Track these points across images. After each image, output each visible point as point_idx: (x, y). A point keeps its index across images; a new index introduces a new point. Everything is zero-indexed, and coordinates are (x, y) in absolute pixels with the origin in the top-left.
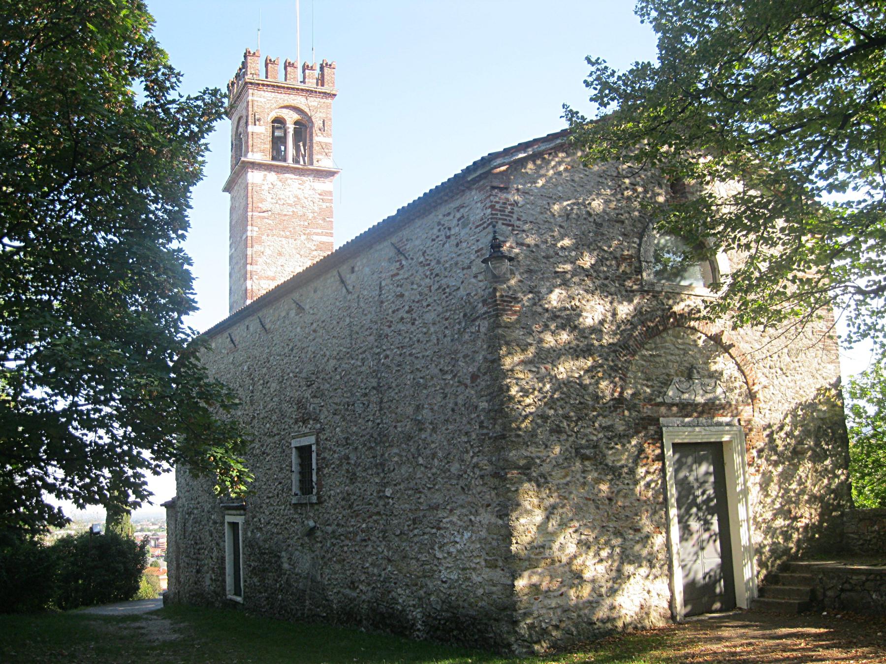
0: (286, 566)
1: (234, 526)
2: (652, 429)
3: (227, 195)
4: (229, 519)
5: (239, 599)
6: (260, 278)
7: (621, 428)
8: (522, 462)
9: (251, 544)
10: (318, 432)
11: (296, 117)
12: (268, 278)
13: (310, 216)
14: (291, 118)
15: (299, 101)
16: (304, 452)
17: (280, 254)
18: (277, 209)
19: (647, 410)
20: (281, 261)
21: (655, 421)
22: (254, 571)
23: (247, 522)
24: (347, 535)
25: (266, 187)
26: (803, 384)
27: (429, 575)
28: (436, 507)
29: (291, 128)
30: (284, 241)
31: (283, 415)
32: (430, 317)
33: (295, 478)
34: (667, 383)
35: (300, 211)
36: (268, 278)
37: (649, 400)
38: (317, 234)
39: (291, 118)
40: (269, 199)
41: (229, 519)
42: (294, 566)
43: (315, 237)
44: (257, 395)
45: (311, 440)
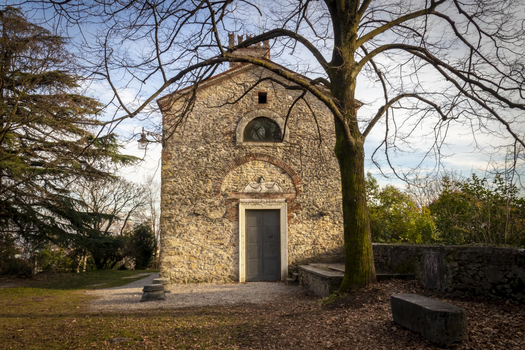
2: (234, 204)
7: (217, 203)
8: (167, 216)
19: (234, 196)
26: (331, 183)
37: (236, 192)
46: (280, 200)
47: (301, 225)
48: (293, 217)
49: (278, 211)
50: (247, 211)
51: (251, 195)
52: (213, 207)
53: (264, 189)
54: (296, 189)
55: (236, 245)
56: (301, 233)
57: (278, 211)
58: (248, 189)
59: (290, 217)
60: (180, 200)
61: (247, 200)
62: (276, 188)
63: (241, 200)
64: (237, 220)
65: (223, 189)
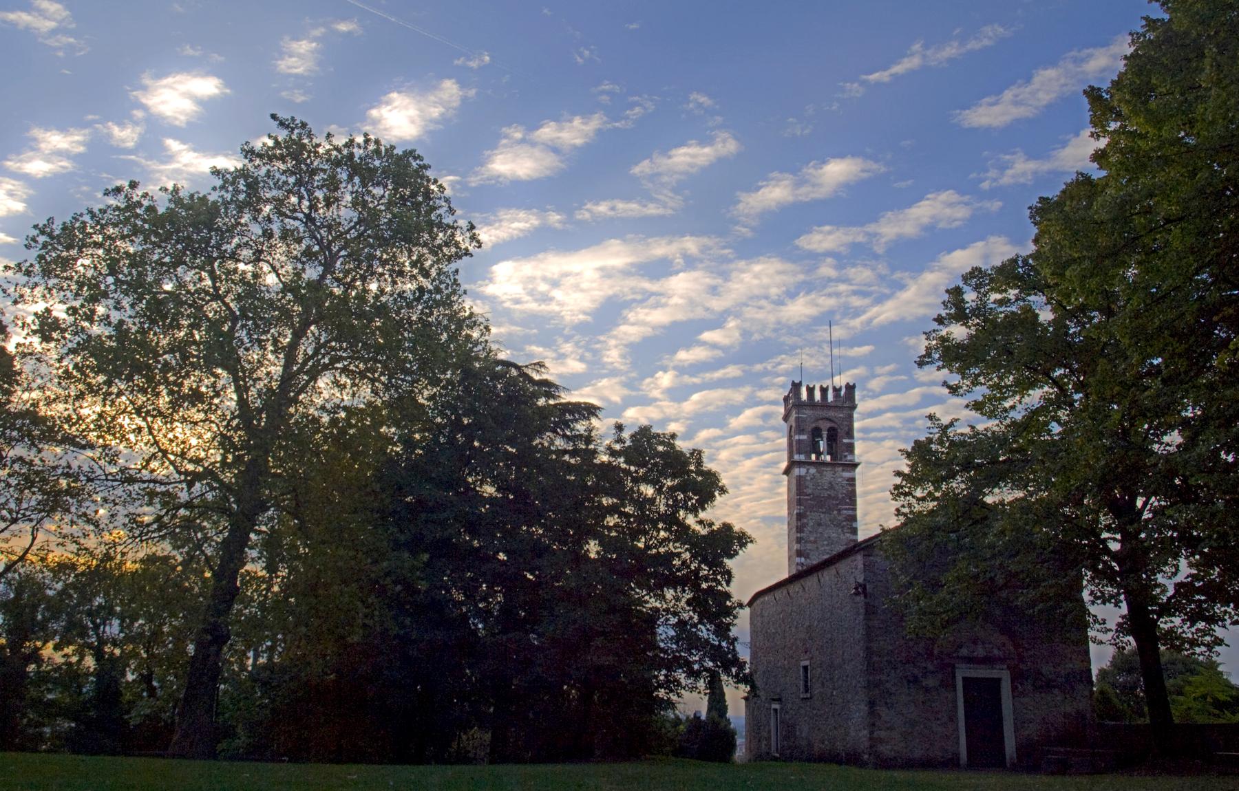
0: (798, 733)
1: (776, 710)
3: (785, 477)
5: (778, 755)
7: (931, 667)
9: (782, 722)
10: (812, 658)
11: (829, 425)
12: (811, 542)
13: (840, 496)
15: (831, 414)
16: (805, 668)
17: (820, 525)
19: (947, 661)
20: (820, 530)
21: (953, 667)
22: (786, 738)
25: (808, 478)
29: (825, 434)
30: (822, 516)
32: (847, 608)
33: (802, 683)
35: (832, 493)
36: (811, 542)
39: (825, 426)
40: (811, 486)
42: (801, 733)
44: (787, 634)
45: (807, 663)
46: (1001, 667)
47: (1026, 700)
48: (1017, 688)
49: (999, 680)
50: (964, 679)
51: (970, 660)
52: (926, 673)
53: (980, 652)
55: (953, 719)
56: (1026, 708)
57: (999, 680)
58: (964, 652)
59: (1014, 689)
60: (889, 662)
61: (964, 666)
62: (996, 652)
63: (957, 665)
64: (955, 690)
65: (936, 652)
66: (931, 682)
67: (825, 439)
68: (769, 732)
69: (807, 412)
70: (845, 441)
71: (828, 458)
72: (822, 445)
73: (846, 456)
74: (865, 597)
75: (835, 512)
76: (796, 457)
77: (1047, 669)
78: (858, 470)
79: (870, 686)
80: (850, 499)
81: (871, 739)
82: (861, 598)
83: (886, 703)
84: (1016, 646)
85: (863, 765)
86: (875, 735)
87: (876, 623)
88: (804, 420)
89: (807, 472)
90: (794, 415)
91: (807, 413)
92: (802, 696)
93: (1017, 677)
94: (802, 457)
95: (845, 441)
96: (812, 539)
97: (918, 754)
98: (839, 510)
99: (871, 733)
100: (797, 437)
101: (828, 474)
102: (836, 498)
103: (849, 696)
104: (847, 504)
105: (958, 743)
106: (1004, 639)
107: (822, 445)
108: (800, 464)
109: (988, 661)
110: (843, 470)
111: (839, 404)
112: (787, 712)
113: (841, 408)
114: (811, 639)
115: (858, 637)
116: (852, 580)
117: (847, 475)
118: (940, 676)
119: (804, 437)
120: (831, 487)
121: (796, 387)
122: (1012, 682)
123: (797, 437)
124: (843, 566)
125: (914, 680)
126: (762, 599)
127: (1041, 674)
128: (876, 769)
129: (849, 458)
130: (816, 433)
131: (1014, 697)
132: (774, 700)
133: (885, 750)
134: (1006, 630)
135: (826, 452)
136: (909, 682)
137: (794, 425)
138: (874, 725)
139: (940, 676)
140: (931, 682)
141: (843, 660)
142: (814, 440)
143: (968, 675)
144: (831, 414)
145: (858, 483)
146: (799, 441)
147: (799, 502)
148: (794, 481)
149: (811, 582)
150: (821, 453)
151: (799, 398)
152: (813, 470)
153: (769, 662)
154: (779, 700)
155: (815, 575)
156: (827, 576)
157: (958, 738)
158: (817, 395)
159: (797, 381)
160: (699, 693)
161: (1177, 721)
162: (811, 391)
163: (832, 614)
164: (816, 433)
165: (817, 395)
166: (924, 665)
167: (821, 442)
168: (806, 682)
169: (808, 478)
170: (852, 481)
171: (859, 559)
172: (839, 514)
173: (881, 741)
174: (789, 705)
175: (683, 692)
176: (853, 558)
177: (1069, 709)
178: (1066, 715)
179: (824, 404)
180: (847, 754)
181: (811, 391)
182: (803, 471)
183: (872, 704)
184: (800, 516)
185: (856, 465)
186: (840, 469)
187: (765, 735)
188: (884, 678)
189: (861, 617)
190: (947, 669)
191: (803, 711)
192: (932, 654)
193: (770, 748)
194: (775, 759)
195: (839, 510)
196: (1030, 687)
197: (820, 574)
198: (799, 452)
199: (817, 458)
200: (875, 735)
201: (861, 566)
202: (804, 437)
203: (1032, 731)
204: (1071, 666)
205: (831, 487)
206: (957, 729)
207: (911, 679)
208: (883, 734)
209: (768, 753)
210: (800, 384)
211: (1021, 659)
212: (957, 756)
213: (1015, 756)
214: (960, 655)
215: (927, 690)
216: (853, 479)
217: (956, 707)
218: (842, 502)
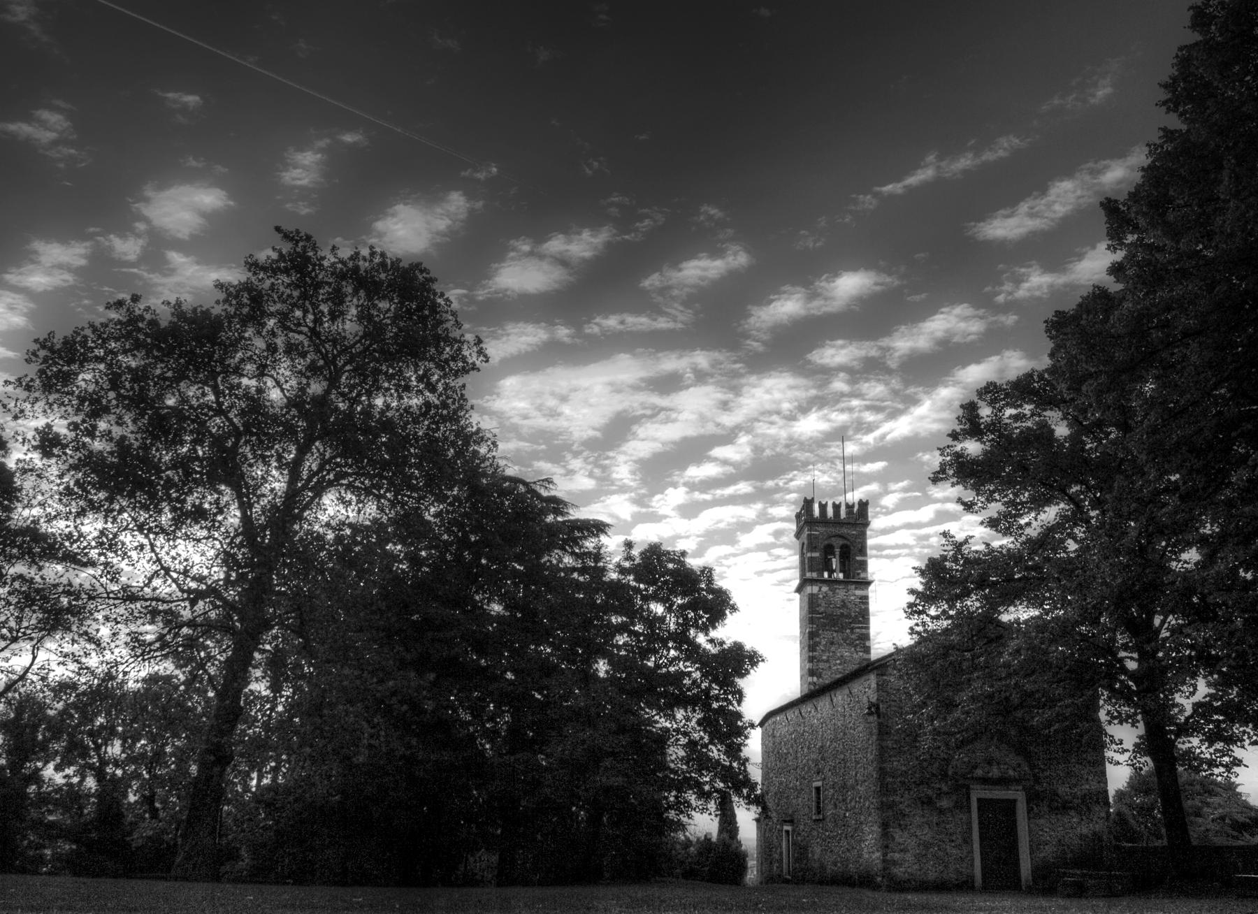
1: (787, 832)
3: (797, 596)
4: (786, 828)
6: (818, 661)
7: (945, 788)
11: (841, 542)
13: (853, 614)
14: (837, 543)
15: (844, 531)
16: (818, 789)
17: (832, 643)
18: (829, 611)
20: (833, 649)
21: (968, 788)
22: (797, 860)
23: (794, 831)
24: (834, 837)
25: (821, 596)
27: (860, 856)
28: (861, 823)
29: (837, 551)
30: (835, 635)
31: (809, 768)
34: (975, 767)
35: (845, 611)
37: (964, 776)
38: (859, 628)
39: (837, 543)
40: (823, 604)
41: (786, 828)
43: (858, 630)
44: (799, 755)
45: (819, 784)
46: (1017, 788)
47: (1042, 821)
48: (1032, 809)
49: (1015, 801)
50: (979, 800)
51: (985, 781)
52: (940, 794)
53: (995, 772)
54: (1034, 775)
55: (967, 841)
56: (1042, 830)
59: (1030, 810)
60: (903, 783)
61: (978, 787)
62: (1011, 772)
64: (970, 812)
65: (950, 773)
66: (945, 803)
67: (838, 556)
68: (781, 853)
69: (820, 529)
70: (858, 558)
71: (841, 576)
72: (835, 563)
73: (858, 574)
74: (879, 717)
75: (848, 631)
76: (808, 575)
77: (1063, 790)
78: (871, 588)
79: (883, 807)
80: (863, 617)
81: (884, 861)
82: (873, 718)
83: (900, 825)
84: (1032, 767)
85: (876, 887)
86: (888, 857)
87: (889, 743)
88: (816, 537)
89: (820, 590)
90: (806, 532)
91: (819, 531)
92: (814, 818)
93: (1033, 798)
94: (815, 575)
95: (858, 558)
96: (824, 658)
97: (932, 876)
98: (852, 629)
99: (885, 855)
100: (809, 555)
101: (841, 594)
102: (849, 616)
103: (862, 818)
104: (860, 622)
105: (972, 865)
106: (1020, 759)
107: (835, 563)
108: (812, 582)
109: (1003, 782)
110: (856, 588)
111: (852, 521)
112: (799, 834)
113: (854, 525)
114: (823, 759)
115: (871, 757)
116: (865, 699)
117: (859, 593)
118: (954, 797)
119: (816, 555)
120: (844, 605)
121: (808, 504)
122: (1028, 803)
123: (809, 555)
124: (857, 687)
125: (928, 802)
126: (773, 719)
127: (1057, 795)
128: (889, 891)
129: (862, 575)
130: (829, 550)
131: (1029, 819)
132: (785, 821)
133: (898, 871)
134: (1021, 750)
135: (838, 570)
136: (923, 803)
137: (806, 542)
138: (887, 847)
139: (954, 797)
140: (945, 803)
141: (856, 781)
142: (826, 558)
143: (979, 796)
144: (844, 531)
145: (871, 601)
146: (811, 559)
147: (811, 621)
148: (806, 599)
149: (824, 704)
150: (834, 571)
151: (812, 515)
152: (825, 589)
153: (781, 783)
154: (791, 822)
155: (828, 694)
156: (840, 697)
157: (973, 860)
158: (830, 512)
159: (809, 498)
160: (710, 814)
161: (1195, 843)
162: (823, 507)
163: (845, 734)
164: (829, 550)
165: (830, 512)
166: (938, 786)
167: (834, 560)
168: (818, 803)
169: (821, 596)
170: (865, 600)
171: (872, 680)
172: (852, 633)
173: (894, 863)
174: (802, 827)
175: (693, 813)
176: (866, 677)
177: (1085, 831)
178: (1082, 837)
179: (837, 521)
180: (859, 877)
181: (823, 507)
182: (815, 589)
183: (885, 826)
184: (812, 635)
185: (868, 583)
186: (853, 587)
187: (777, 856)
188: (898, 799)
189: (875, 737)
190: (961, 789)
191: (815, 833)
192: (946, 775)
193: (782, 871)
194: (787, 881)
195: (852, 629)
196: (1046, 809)
197: (832, 693)
198: (811, 570)
199: (830, 576)
200: (888, 857)
201: (874, 685)
202: (816, 555)
203: (1048, 852)
204: (1088, 787)
205: (844, 605)
206: (972, 851)
207: (926, 800)
208: (897, 856)
209: (779, 876)
210: (812, 501)
211: (1037, 780)
212: (972, 877)
213: (1030, 878)
214: (975, 775)
215: (941, 812)
216: (866, 597)
217: (970, 829)
218: (855, 620)
